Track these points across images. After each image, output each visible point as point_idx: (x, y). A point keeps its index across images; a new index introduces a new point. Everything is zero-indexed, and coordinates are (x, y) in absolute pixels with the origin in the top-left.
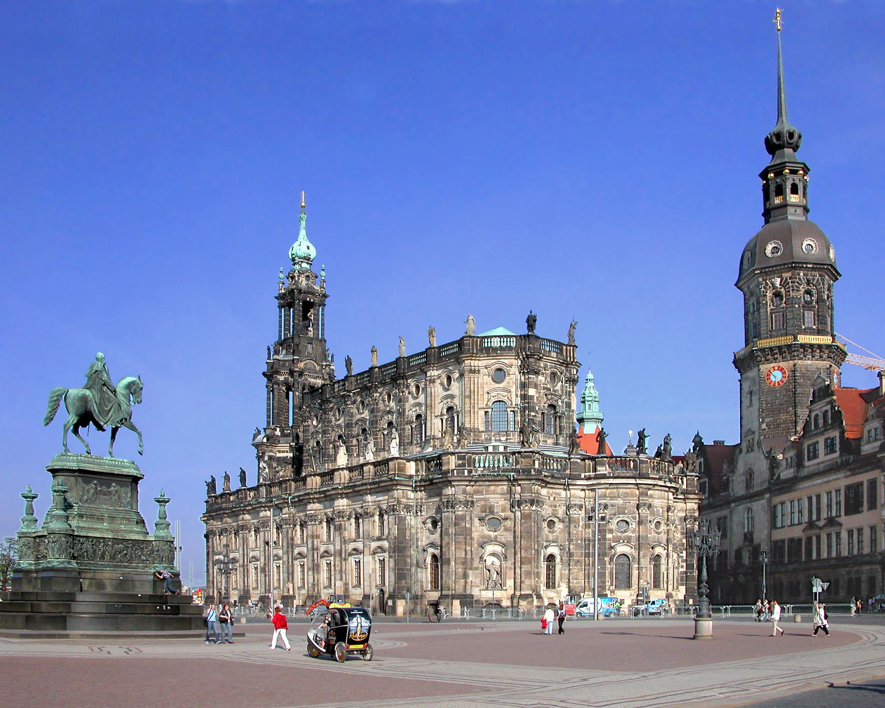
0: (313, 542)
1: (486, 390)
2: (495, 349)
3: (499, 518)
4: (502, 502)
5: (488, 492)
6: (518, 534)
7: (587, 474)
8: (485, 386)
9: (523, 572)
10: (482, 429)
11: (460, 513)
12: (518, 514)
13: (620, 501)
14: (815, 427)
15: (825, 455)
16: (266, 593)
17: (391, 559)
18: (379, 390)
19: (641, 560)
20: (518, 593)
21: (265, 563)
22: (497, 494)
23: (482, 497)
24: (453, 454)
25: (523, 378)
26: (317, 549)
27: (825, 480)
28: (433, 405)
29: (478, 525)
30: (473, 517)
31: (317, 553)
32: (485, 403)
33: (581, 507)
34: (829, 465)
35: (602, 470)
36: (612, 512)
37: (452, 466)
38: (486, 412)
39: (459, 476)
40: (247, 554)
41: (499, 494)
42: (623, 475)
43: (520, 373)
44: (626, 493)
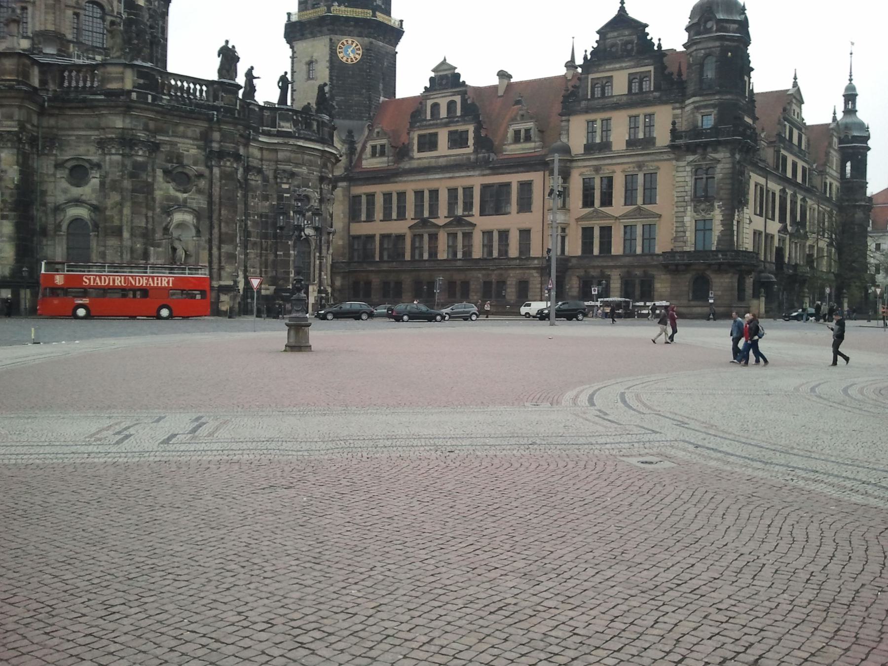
3: (191, 174)
4: (194, 151)
5: (175, 135)
6: (216, 199)
7: (264, 128)
9: (223, 254)
10: (70, 37)
11: (140, 159)
12: (216, 171)
13: (304, 170)
14: (432, 115)
15: (449, 148)
19: (323, 248)
20: (215, 284)
22: (187, 138)
23: (167, 139)
24: (133, 66)
27: (448, 175)
30: (155, 167)
33: (260, 171)
34: (455, 160)
35: (287, 127)
36: (296, 183)
37: (128, 86)
38: (77, 15)
39: (141, 103)
41: (190, 138)
42: (308, 137)
44: (310, 161)
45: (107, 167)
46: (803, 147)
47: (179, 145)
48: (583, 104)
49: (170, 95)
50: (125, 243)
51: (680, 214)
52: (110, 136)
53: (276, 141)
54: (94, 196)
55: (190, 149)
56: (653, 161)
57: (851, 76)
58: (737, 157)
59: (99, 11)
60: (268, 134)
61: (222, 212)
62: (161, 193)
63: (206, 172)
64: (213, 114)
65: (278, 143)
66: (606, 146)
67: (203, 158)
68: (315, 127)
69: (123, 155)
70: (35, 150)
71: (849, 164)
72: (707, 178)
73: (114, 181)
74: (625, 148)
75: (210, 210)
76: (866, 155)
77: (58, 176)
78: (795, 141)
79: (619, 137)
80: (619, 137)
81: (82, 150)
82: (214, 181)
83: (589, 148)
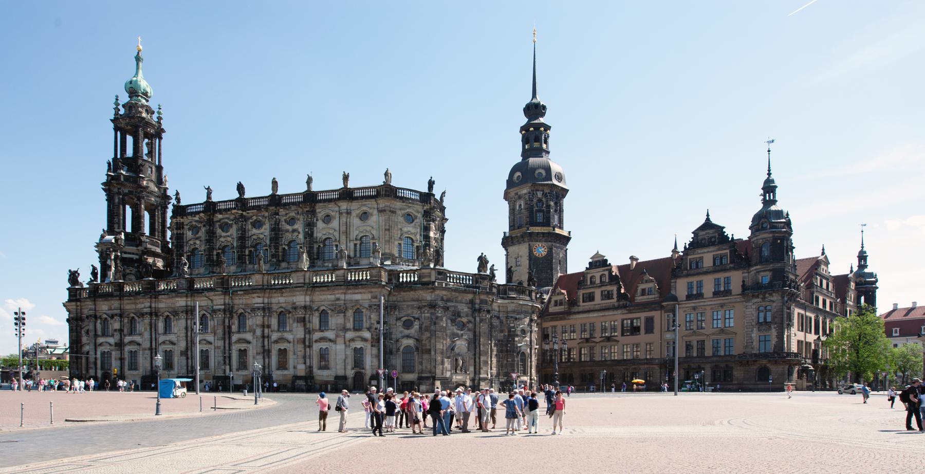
0: (263, 331)
1: (399, 227)
2: (408, 199)
4: (466, 310)
5: (457, 302)
8: (399, 224)
10: (397, 255)
12: (478, 319)
16: (188, 373)
17: (373, 348)
18: (280, 214)
21: (187, 348)
22: (463, 303)
25: (425, 223)
26: (268, 337)
28: (348, 232)
29: (450, 325)
31: (268, 340)
32: (399, 236)
40: (156, 340)
43: (423, 219)
45: (423, 320)
46: (830, 290)
47: (459, 307)
48: (685, 272)
49: (453, 282)
50: (432, 357)
51: (749, 333)
52: (424, 304)
53: (507, 302)
54: (416, 334)
55: (464, 309)
56: (730, 303)
57: (862, 245)
58: (786, 299)
59: (410, 241)
60: (503, 298)
61: (481, 340)
62: (450, 331)
63: (473, 320)
64: (476, 291)
65: (508, 303)
66: (700, 296)
67: (471, 313)
68: (527, 293)
69: (431, 313)
70: (386, 313)
71: (863, 299)
72: (766, 312)
73: (426, 326)
74: (712, 296)
75: (475, 339)
76: (875, 292)
77: (398, 325)
78: (824, 286)
79: (708, 288)
80: (708, 288)
81: (410, 312)
82: (477, 324)
83: (689, 297)
